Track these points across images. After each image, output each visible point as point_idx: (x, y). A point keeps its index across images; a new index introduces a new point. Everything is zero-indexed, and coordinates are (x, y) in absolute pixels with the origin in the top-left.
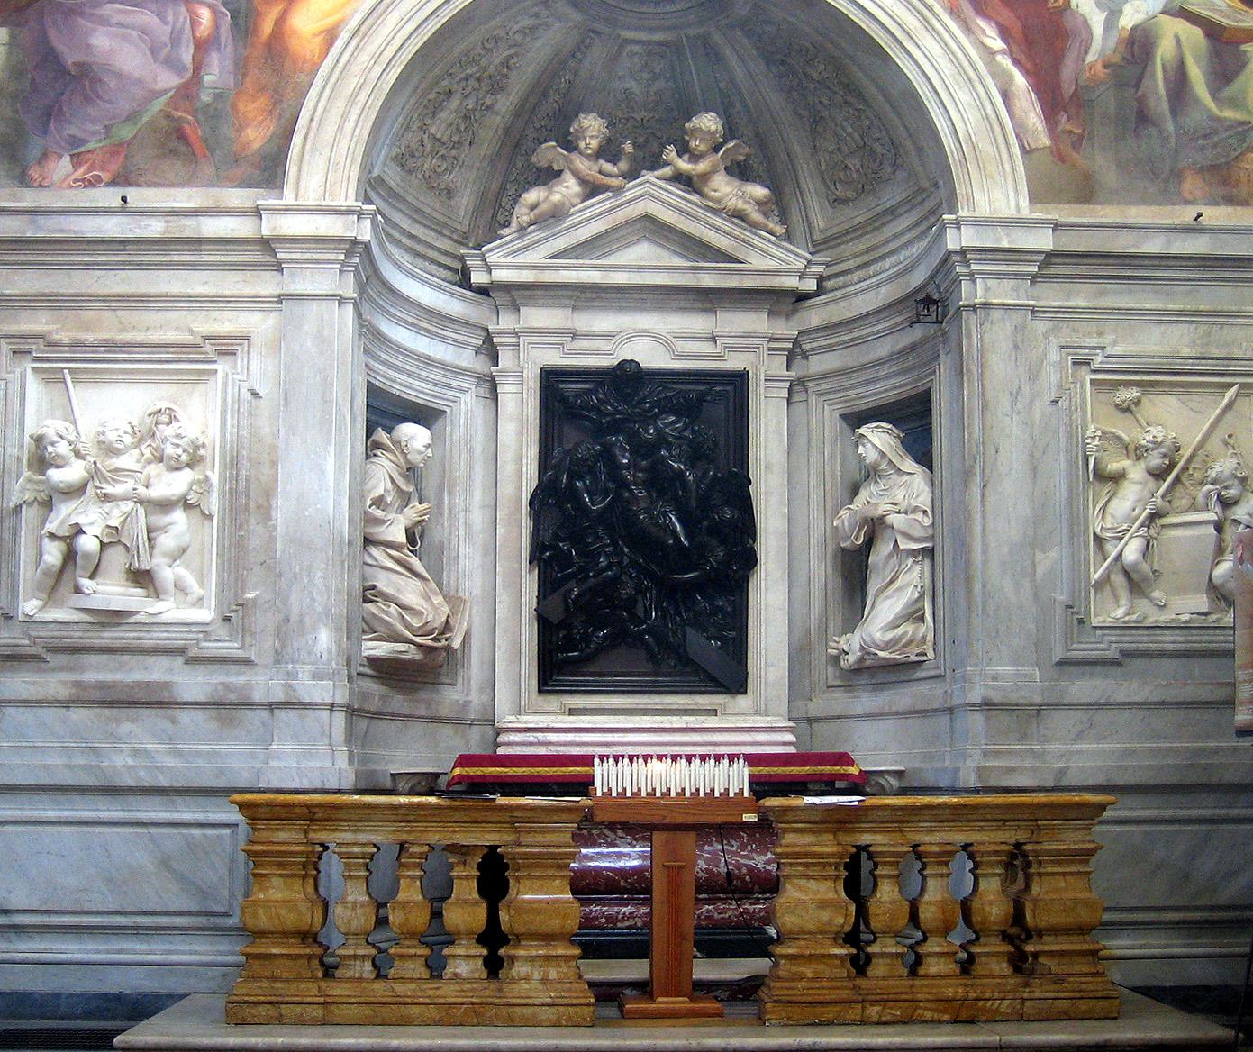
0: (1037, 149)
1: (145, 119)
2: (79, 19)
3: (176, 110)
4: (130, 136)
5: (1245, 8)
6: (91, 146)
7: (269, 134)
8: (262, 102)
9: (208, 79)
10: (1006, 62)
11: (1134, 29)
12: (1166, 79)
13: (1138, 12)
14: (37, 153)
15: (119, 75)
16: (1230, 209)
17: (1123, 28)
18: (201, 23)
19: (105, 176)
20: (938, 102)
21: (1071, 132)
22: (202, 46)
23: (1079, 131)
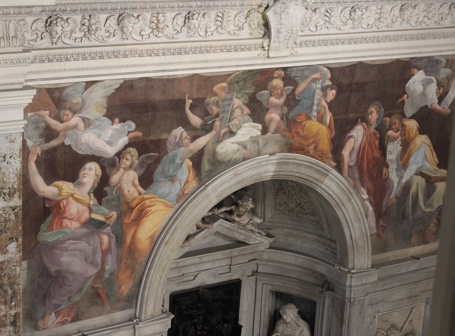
0: (373, 234)
1: (84, 291)
2: (55, 250)
3: (96, 284)
4: (79, 299)
5: (439, 169)
6: (63, 306)
7: (130, 287)
8: (128, 273)
9: (107, 267)
10: (367, 203)
11: (406, 182)
12: (412, 201)
13: (408, 175)
14: (41, 314)
15: (73, 273)
16: (423, 246)
17: (403, 183)
18: (104, 243)
19: (69, 319)
20: (347, 225)
21: (383, 226)
22: (105, 253)
23: (385, 225)
